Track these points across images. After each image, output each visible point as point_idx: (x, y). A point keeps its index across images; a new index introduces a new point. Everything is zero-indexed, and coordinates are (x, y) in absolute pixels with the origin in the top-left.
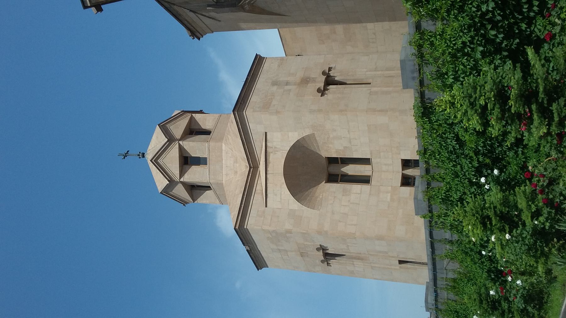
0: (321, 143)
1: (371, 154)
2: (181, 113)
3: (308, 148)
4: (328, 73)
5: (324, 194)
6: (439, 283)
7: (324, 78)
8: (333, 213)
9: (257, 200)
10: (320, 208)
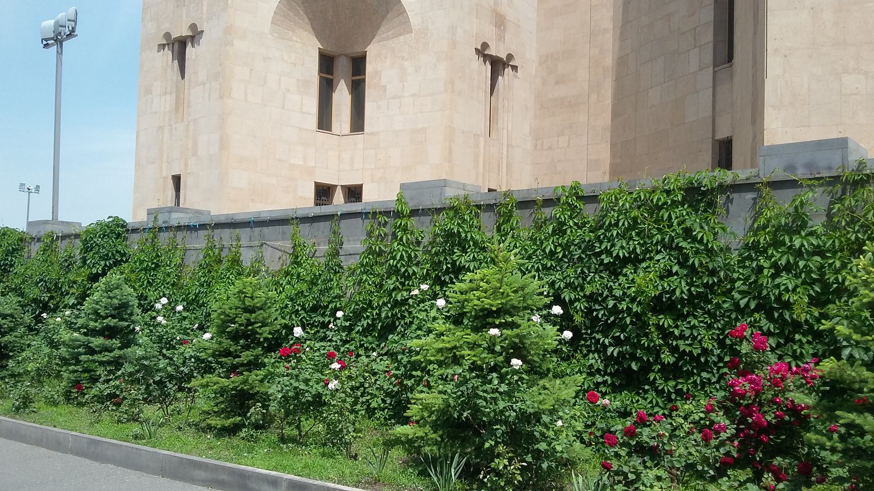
0: (393, 45)
1: (372, 133)
3: (385, 20)
4: (508, 65)
6: (226, 233)
7: (503, 56)
10: (274, 36)
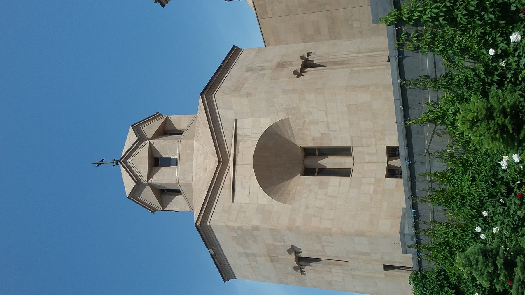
0: (296, 129)
1: (351, 141)
2: (156, 114)
4: (307, 58)
5: (298, 187)
6: (419, 186)
7: (301, 61)
8: (307, 207)
9: (224, 194)
10: (293, 202)
